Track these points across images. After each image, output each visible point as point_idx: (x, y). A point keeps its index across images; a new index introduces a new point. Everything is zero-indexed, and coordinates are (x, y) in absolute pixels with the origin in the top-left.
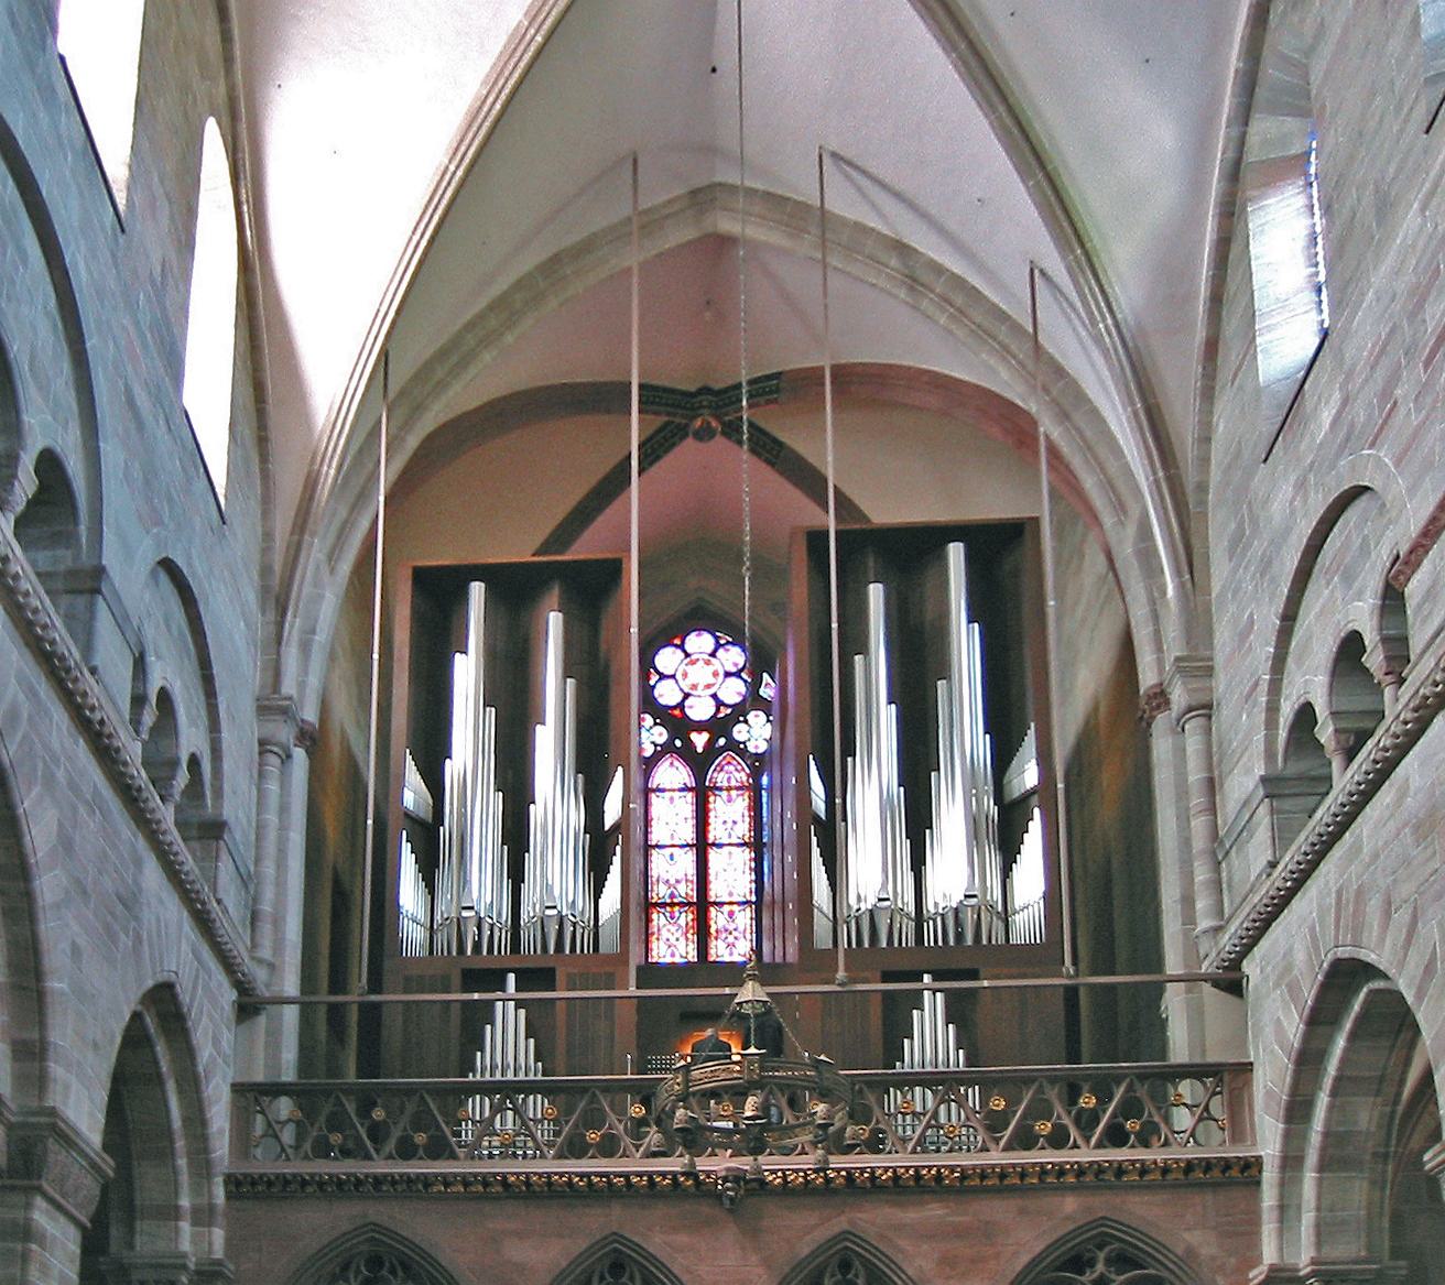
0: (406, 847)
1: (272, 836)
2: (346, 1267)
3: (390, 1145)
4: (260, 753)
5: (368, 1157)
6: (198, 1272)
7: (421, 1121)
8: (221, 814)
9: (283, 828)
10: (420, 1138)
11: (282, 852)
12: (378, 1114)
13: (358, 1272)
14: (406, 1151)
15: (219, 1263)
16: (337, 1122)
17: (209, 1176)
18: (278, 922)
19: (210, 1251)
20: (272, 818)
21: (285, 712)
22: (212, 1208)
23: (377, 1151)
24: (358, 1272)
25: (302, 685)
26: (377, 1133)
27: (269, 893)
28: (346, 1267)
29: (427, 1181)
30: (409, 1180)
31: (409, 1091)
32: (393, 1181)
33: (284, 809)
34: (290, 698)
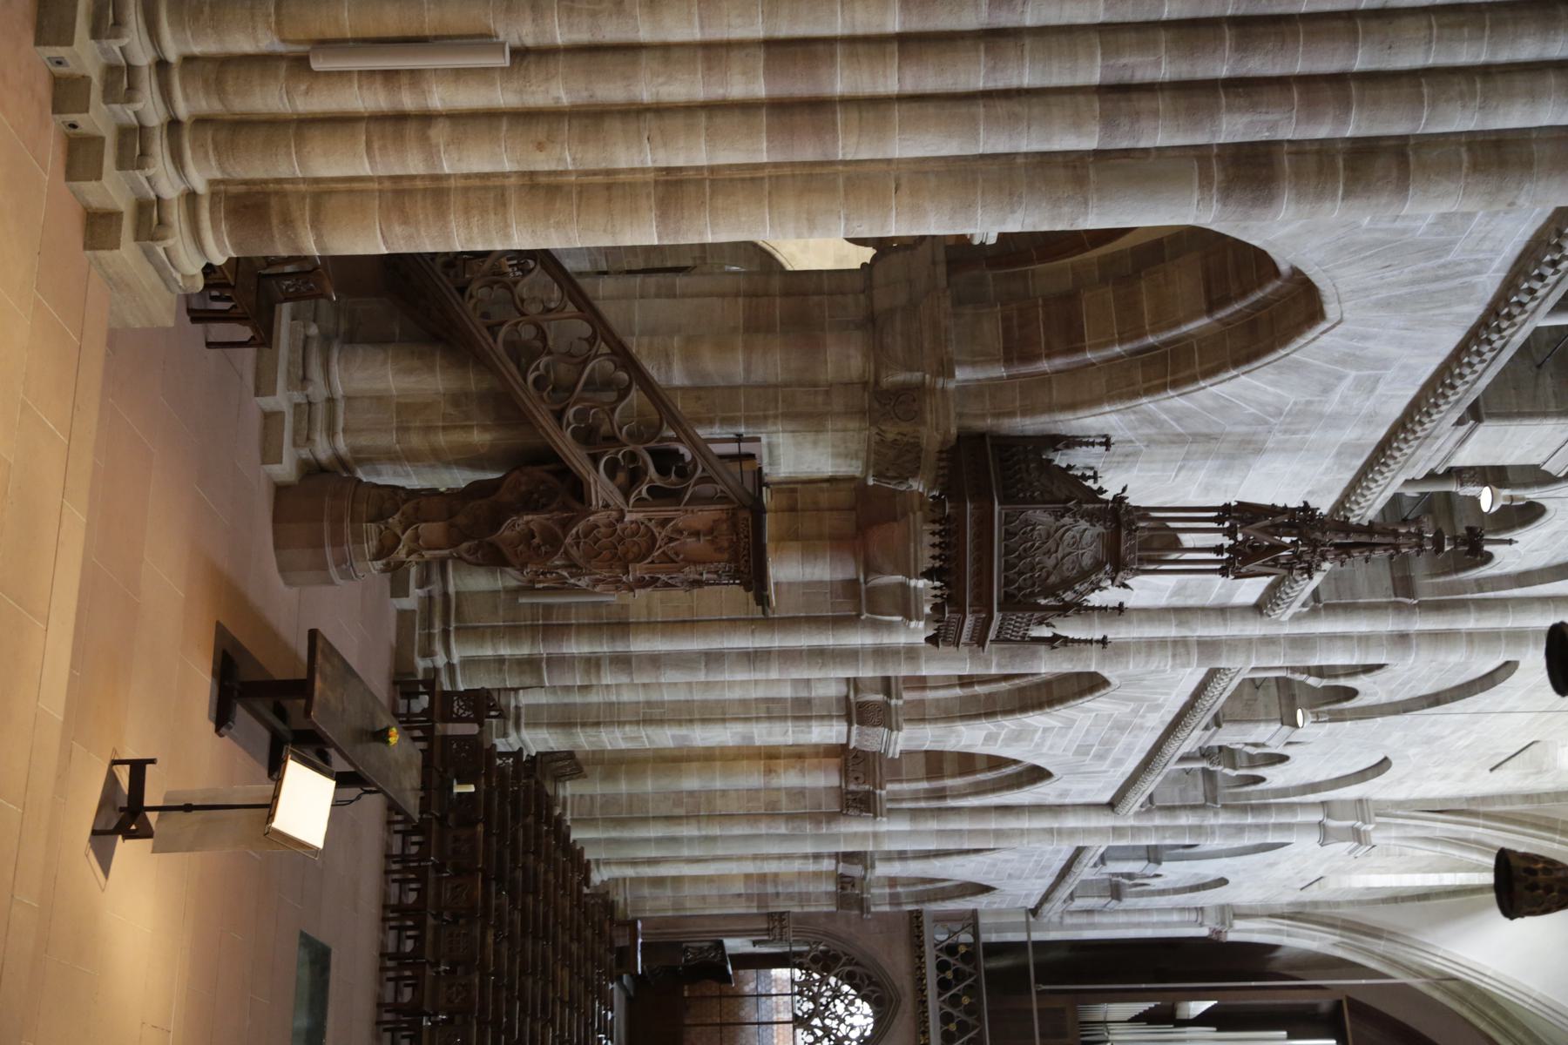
0: (1152, 1005)
1: (1144, 919)
2: (876, 984)
3: (949, 1010)
4: (1196, 908)
5: (940, 995)
6: (862, 899)
7: (963, 1028)
8: (1127, 897)
9: (1154, 925)
10: (953, 1027)
11: (1139, 925)
12: (966, 1000)
13: (874, 992)
14: (946, 1018)
15: (869, 911)
16: (959, 976)
17: (917, 902)
18: (1093, 926)
19: (875, 905)
20: (1155, 918)
21: (1223, 923)
22: (899, 904)
23: (944, 1001)
24: (874, 992)
25: (1238, 931)
26: (955, 1001)
27: (1105, 919)
28: (876, 984)
29: (925, 1032)
30: (925, 1021)
31: (980, 1019)
32: (925, 1012)
33: (1167, 925)
34: (1231, 926)
